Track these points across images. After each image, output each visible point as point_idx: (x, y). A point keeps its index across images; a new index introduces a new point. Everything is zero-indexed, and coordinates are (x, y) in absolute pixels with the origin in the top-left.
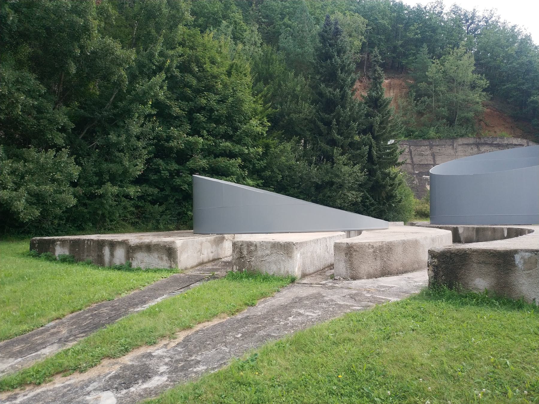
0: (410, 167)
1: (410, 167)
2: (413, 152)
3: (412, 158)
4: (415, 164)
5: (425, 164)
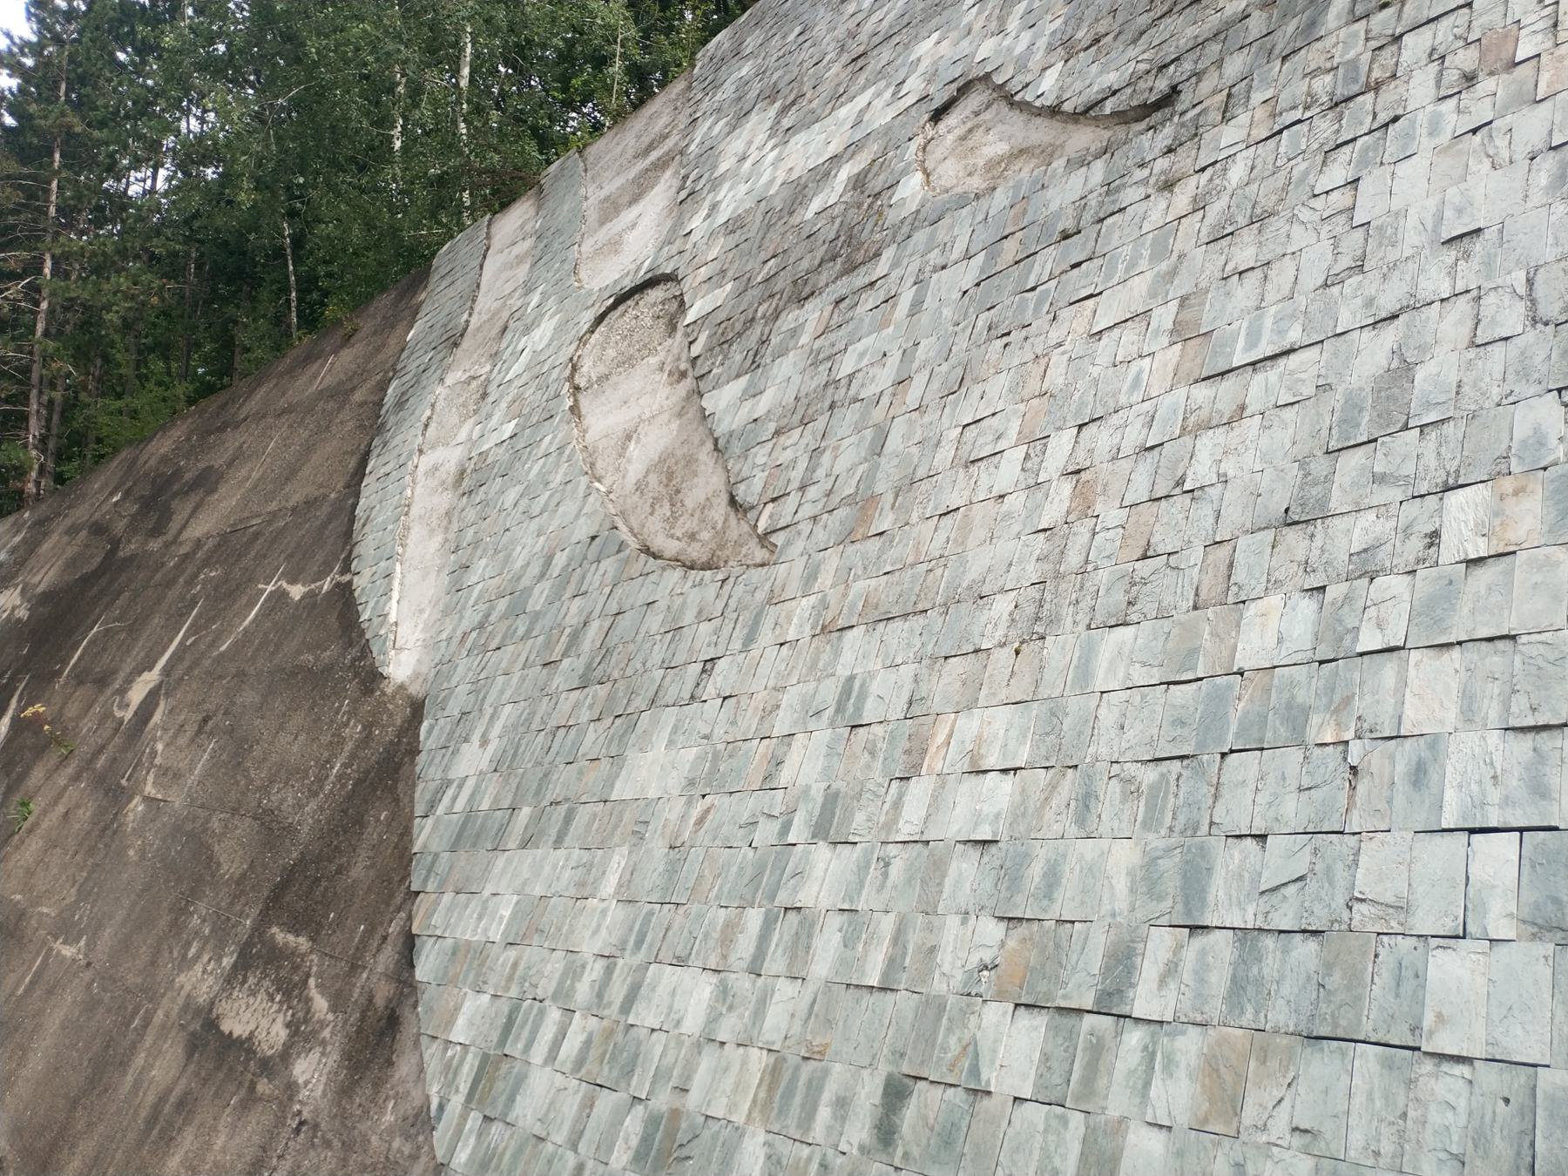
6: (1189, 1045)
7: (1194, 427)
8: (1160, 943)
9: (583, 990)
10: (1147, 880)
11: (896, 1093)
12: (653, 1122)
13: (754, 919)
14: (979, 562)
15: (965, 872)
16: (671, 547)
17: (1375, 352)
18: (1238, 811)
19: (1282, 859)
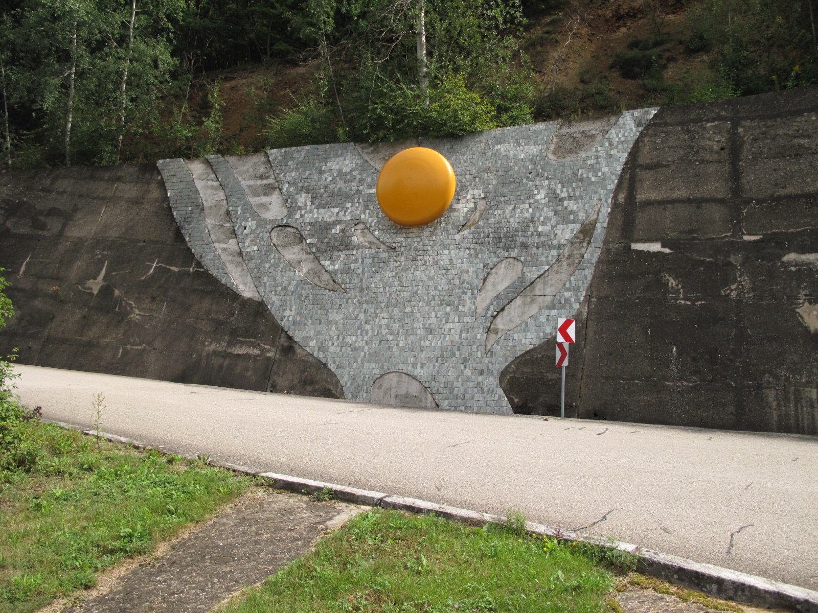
0: (717, 217)
1: (717, 217)
2: (747, 147)
3: (736, 175)
4: (747, 202)
5: (808, 196)
6: (404, 336)
7: (401, 291)
8: (401, 330)
9: (335, 339)
10: (400, 326)
11: (380, 342)
12: (352, 349)
13: (359, 331)
14: (380, 299)
15: (384, 327)
16: (322, 286)
17: (415, 289)
18: (406, 322)
19: (409, 325)
